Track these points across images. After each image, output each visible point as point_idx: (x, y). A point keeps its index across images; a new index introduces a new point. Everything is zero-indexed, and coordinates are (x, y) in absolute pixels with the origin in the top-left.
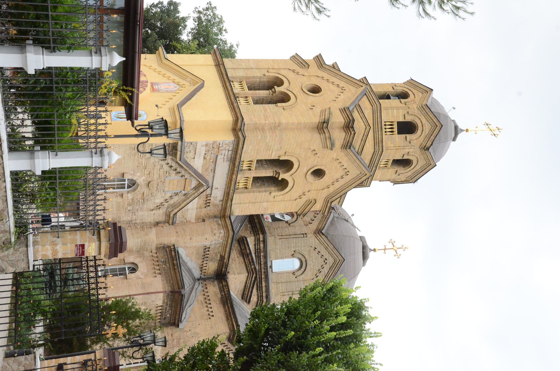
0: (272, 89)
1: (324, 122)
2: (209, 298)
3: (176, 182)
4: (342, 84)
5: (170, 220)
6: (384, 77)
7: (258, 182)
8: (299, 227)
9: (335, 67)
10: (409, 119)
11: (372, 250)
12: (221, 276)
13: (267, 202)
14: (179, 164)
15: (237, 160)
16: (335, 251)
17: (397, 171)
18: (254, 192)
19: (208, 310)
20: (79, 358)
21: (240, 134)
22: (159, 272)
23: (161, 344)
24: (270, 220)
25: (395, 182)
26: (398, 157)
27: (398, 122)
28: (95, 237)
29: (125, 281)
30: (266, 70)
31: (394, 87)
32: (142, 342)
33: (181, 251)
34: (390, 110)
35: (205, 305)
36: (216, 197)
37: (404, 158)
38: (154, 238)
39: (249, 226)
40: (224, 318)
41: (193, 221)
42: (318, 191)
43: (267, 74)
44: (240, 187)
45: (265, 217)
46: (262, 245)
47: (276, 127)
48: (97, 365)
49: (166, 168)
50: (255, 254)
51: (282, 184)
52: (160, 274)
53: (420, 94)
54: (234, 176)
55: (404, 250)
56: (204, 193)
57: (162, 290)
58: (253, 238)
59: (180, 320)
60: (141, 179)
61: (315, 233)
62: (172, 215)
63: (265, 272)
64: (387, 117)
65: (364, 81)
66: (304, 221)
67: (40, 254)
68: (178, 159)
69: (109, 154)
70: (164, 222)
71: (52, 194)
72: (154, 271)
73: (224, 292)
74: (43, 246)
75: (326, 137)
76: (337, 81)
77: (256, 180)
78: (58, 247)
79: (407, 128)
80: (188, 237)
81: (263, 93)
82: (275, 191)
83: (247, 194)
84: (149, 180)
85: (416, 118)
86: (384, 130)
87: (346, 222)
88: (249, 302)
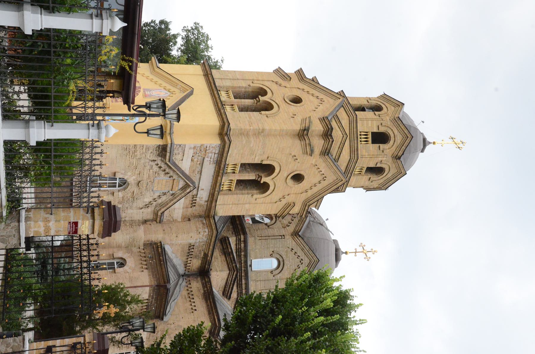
0: (256, 98)
1: (305, 130)
2: (192, 293)
3: (164, 182)
4: (321, 96)
5: (157, 218)
6: (360, 90)
7: (241, 185)
8: (277, 230)
9: (314, 80)
10: (382, 129)
11: (344, 253)
12: (204, 273)
13: (250, 204)
14: (168, 165)
15: (223, 163)
16: (311, 252)
17: (370, 178)
18: (237, 194)
19: (191, 305)
20: (69, 341)
21: (226, 138)
22: (146, 267)
23: (149, 330)
24: (250, 222)
25: (368, 189)
26: (372, 165)
27: (372, 133)
28: (89, 215)
29: (114, 275)
30: (251, 81)
31: (369, 100)
32: (130, 327)
33: (168, 248)
34: (365, 121)
35: (189, 299)
36: (202, 198)
37: (378, 166)
38: (142, 235)
39: (231, 227)
40: (206, 312)
41: (179, 220)
42: (296, 194)
43: (251, 85)
44: (224, 189)
45: (246, 219)
46: (242, 245)
47: (260, 133)
48: (86, 348)
49: (156, 168)
50: (236, 253)
51: (264, 188)
52: (147, 269)
53: (393, 108)
54: (219, 178)
55: (373, 254)
56: (191, 193)
57: (148, 284)
58: (234, 238)
59: (164, 314)
60: (131, 179)
61: (292, 235)
62: (159, 214)
63: (245, 271)
64: (362, 127)
65: (341, 94)
66: (282, 224)
67: (32, 230)
68: (167, 160)
69: (106, 127)
70: (152, 221)
71: (46, 168)
72: (141, 266)
73: (207, 288)
74: (36, 222)
75: (306, 144)
76: (316, 93)
77: (240, 183)
78: (51, 224)
79: (380, 138)
80: (174, 235)
81: (248, 102)
82: (257, 194)
83: (230, 196)
84: (139, 179)
85: (389, 129)
86: (359, 140)
87: (320, 226)
88: (229, 299)
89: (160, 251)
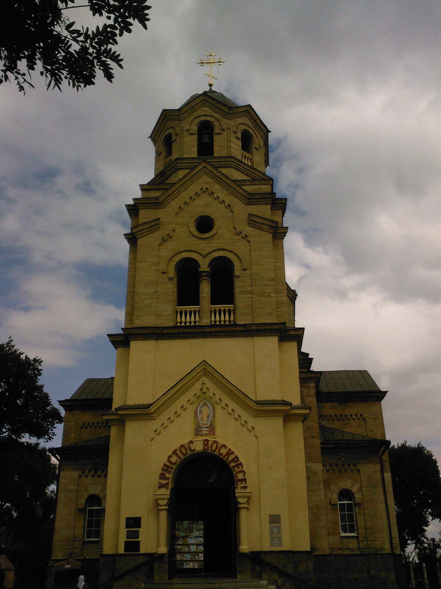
52: (355, 465)
89: (332, 446)
